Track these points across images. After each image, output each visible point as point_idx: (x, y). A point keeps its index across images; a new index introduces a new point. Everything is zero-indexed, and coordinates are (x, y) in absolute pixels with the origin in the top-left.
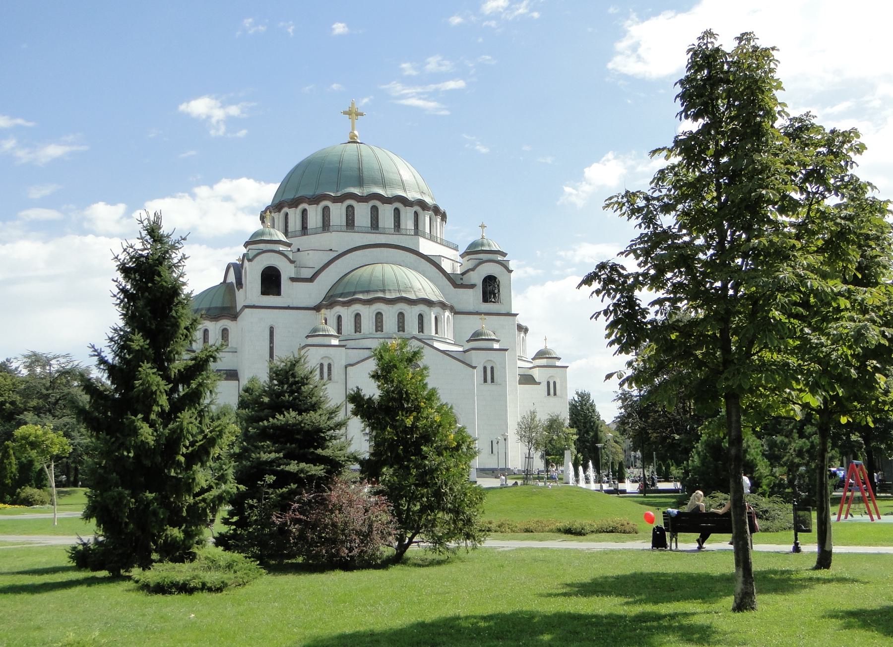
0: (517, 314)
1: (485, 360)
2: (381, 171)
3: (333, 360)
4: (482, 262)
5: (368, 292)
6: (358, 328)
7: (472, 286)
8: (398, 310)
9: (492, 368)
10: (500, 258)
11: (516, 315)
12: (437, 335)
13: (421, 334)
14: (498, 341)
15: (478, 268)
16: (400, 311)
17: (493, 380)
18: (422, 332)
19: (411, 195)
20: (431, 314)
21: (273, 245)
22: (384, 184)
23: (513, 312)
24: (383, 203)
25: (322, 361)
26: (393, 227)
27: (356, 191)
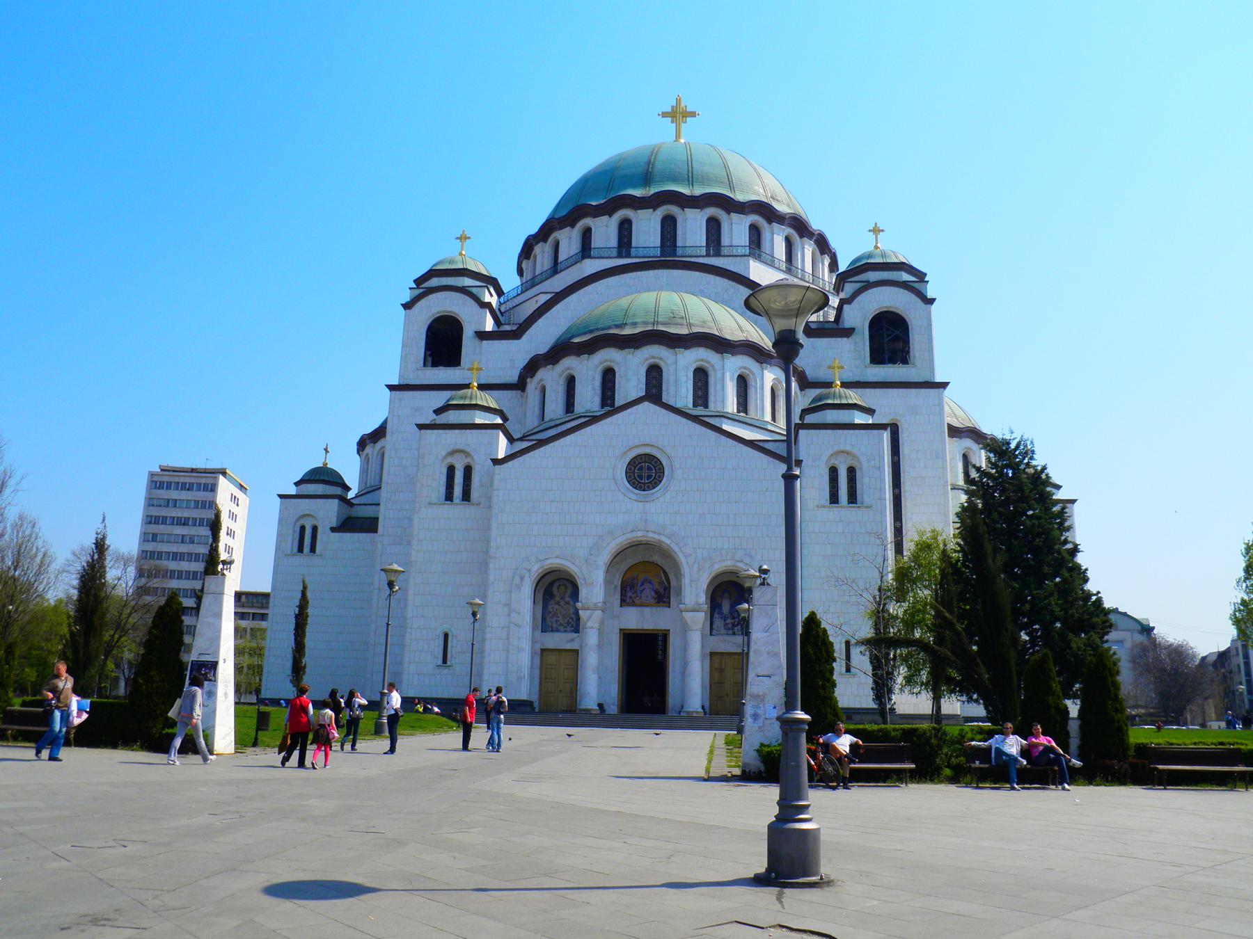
0: (948, 383)
1: (830, 452)
2: (690, 162)
3: (472, 457)
4: (869, 285)
5: (591, 332)
6: (569, 405)
7: (848, 332)
8: (647, 359)
9: (852, 472)
10: (906, 277)
11: (944, 385)
12: (742, 414)
13: (699, 411)
14: (870, 411)
15: (859, 298)
16: (652, 361)
17: (853, 498)
18: (706, 406)
19: (740, 197)
20: (727, 370)
21: (453, 279)
22: (690, 180)
23: (938, 379)
24: (683, 207)
25: (450, 460)
26: (705, 245)
27: (638, 192)
